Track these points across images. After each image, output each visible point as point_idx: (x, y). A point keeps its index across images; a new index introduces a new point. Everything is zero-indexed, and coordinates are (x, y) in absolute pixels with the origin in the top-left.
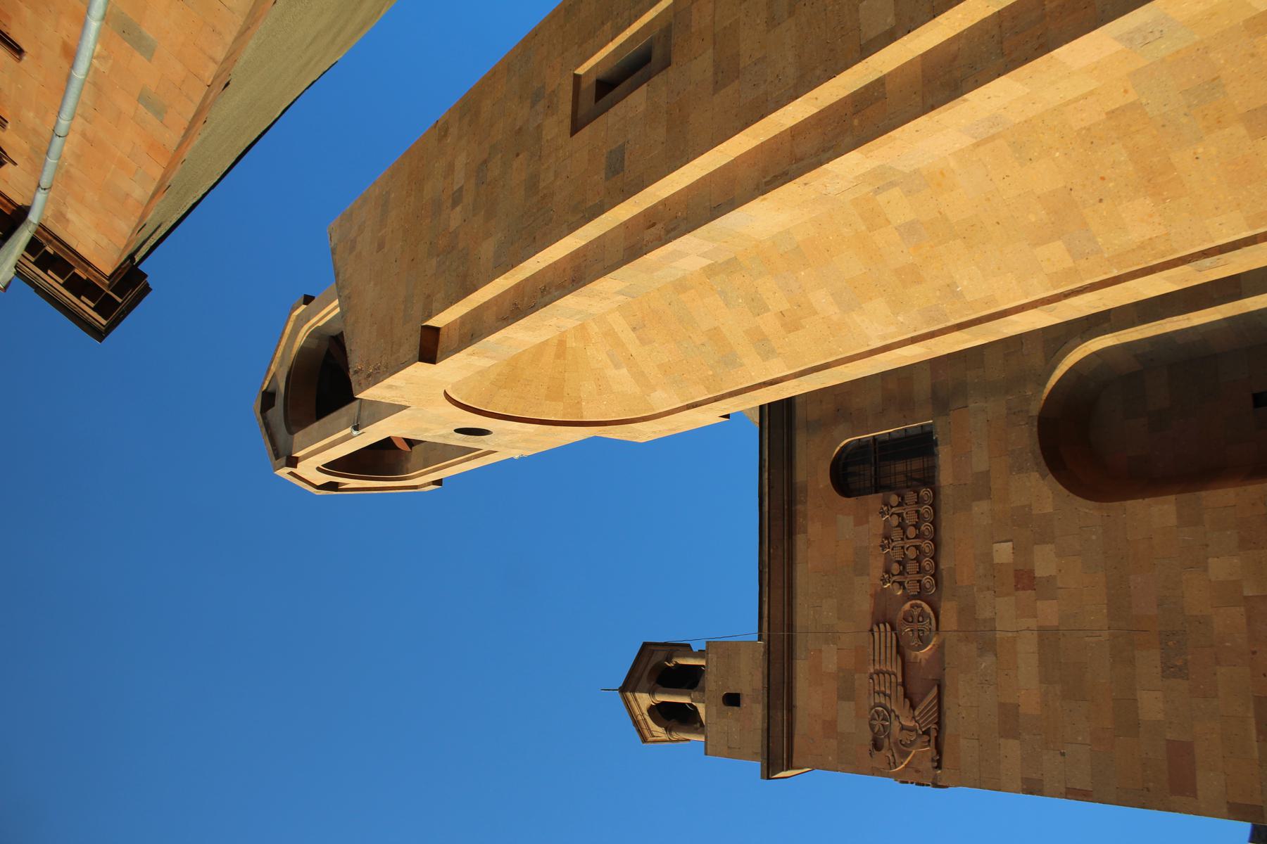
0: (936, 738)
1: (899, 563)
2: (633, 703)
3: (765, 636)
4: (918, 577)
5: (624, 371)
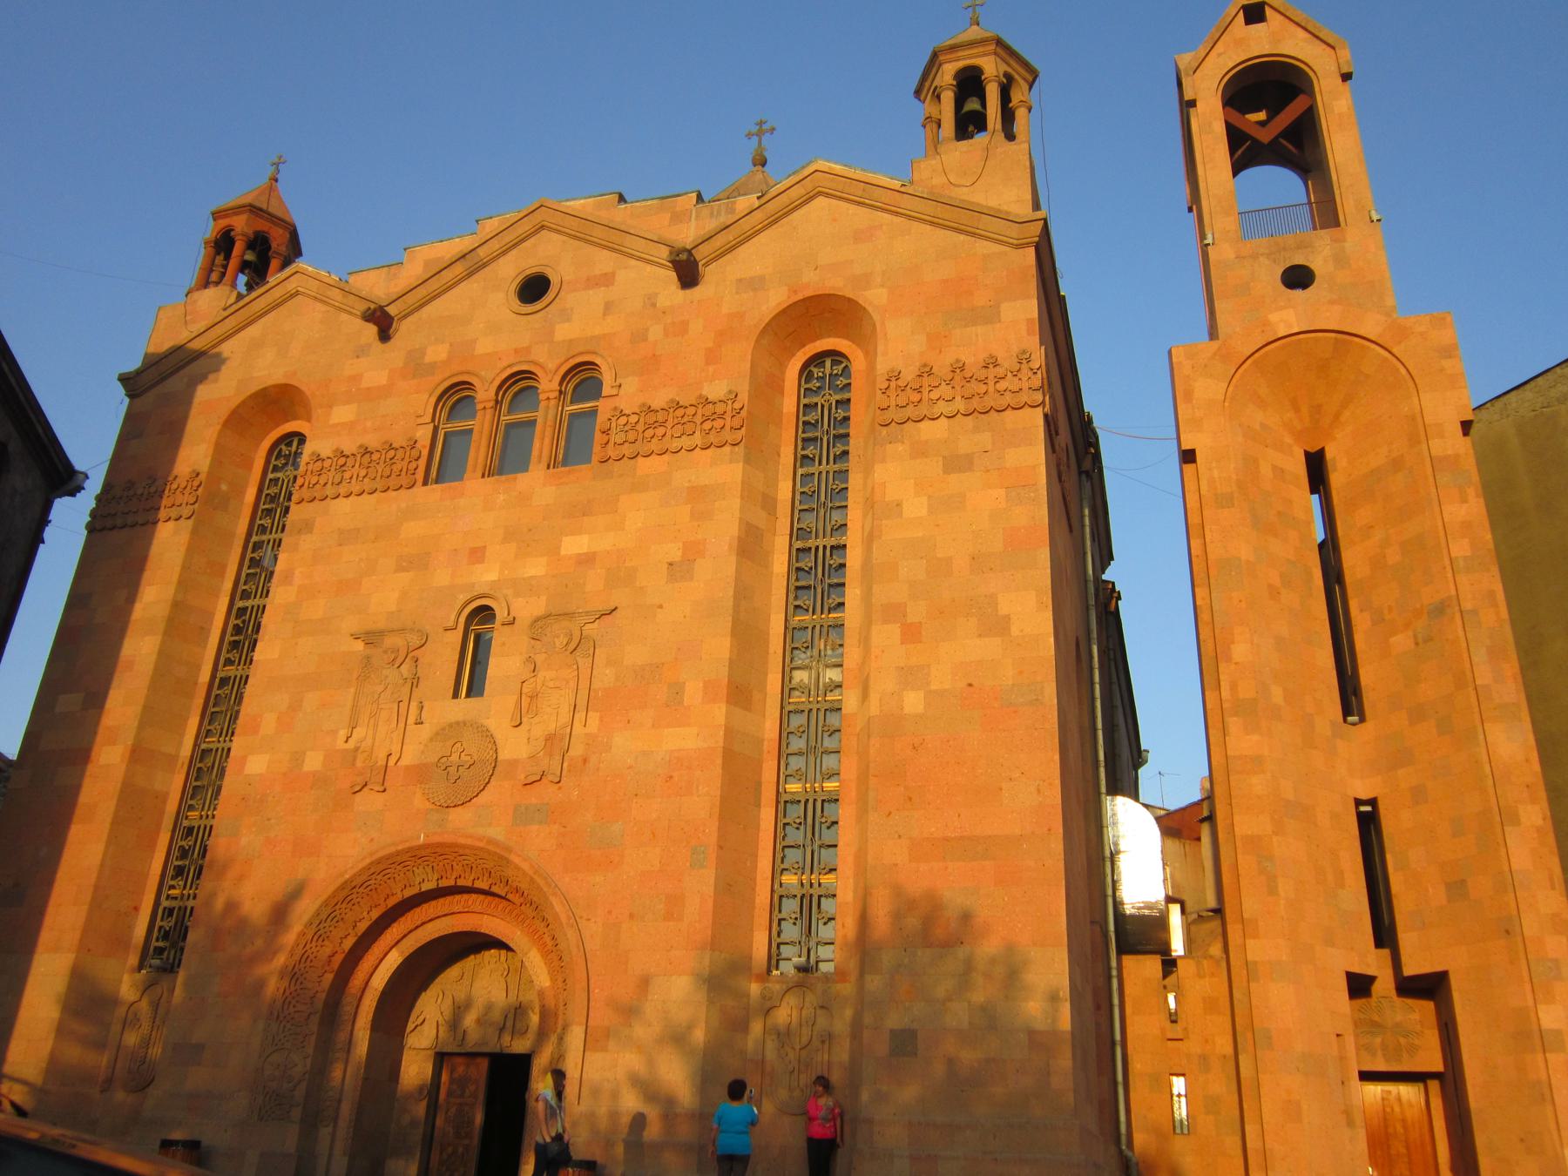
5: (1257, 427)
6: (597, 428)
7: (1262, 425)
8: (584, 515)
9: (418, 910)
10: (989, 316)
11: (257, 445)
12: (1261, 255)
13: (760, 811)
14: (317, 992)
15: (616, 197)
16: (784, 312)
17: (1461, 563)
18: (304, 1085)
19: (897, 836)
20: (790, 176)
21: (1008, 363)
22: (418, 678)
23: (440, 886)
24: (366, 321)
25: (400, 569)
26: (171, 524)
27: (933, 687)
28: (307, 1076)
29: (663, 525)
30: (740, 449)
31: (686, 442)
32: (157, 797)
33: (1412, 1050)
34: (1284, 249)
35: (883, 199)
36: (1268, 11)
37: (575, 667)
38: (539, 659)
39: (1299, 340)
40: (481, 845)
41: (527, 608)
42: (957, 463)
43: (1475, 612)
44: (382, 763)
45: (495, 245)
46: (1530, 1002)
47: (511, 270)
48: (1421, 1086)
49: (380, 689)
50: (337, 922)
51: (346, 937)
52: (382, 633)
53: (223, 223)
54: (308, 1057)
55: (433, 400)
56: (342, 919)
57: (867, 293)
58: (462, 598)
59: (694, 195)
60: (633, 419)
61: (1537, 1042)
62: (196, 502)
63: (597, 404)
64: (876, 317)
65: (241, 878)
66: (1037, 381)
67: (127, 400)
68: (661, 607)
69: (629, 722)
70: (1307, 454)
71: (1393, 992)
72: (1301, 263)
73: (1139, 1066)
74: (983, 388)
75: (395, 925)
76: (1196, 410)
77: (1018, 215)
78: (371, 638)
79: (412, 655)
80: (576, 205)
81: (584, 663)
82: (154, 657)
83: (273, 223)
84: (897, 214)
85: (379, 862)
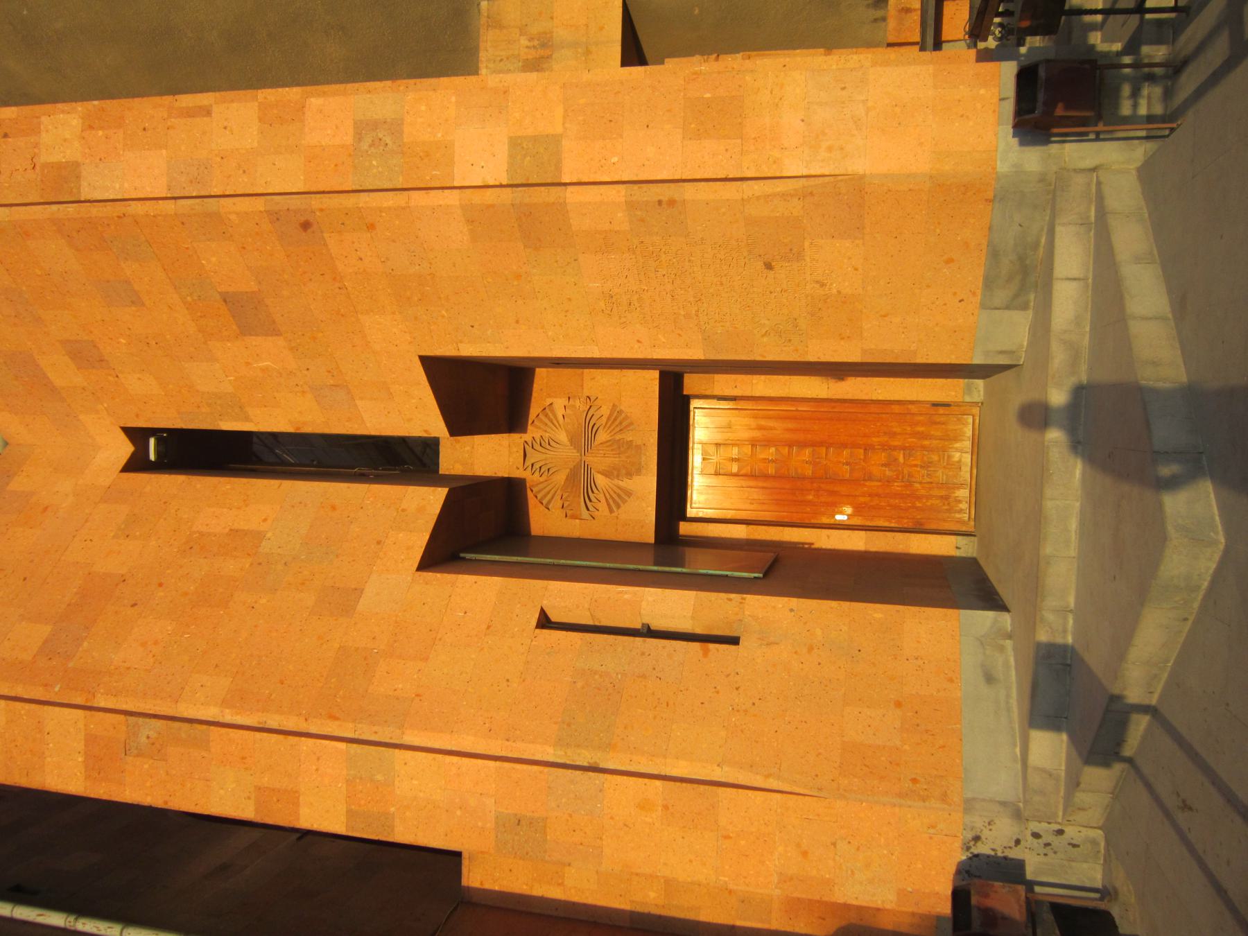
33: (618, 419)
46: (452, 198)
48: (694, 403)
61: (541, 195)
71: (516, 439)
73: (652, 895)
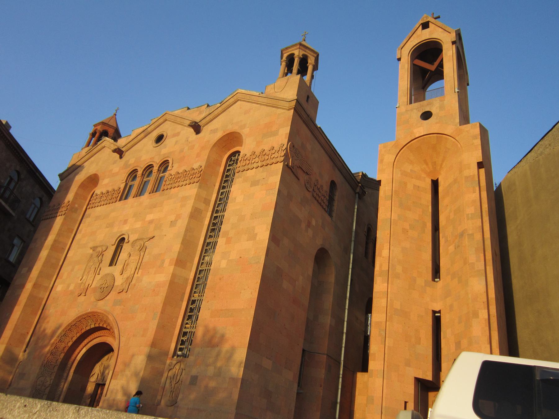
0: (291, 170)
1: (319, 189)
2: (312, 54)
3: (319, 129)
4: (316, 192)
5: (409, 171)
6: (164, 180)
7: (411, 170)
8: (154, 208)
9: (92, 335)
10: (275, 134)
11: (90, 193)
12: (415, 109)
13: (182, 303)
14: (58, 359)
15: (187, 108)
16: (221, 139)
17: (470, 216)
18: (49, 388)
19: (208, 309)
20: (230, 95)
21: (276, 148)
22: (102, 260)
23: (96, 326)
24: (114, 152)
25: (107, 227)
26: (60, 217)
27: (230, 259)
28: (50, 385)
29: (173, 210)
30: (198, 184)
31: (184, 183)
32: (40, 299)
34: (423, 106)
35: (254, 100)
36: (430, 24)
37: (139, 255)
38: (131, 253)
39: (424, 138)
40: (102, 312)
41: (133, 238)
42: (255, 183)
43: (472, 234)
44: (87, 287)
45: (153, 127)
47: (155, 134)
49: (92, 264)
50: (67, 337)
51: (69, 342)
52: (97, 247)
53: (96, 128)
54: (52, 379)
55: (127, 175)
56: (68, 336)
57: (243, 130)
58: (119, 235)
59: (207, 105)
60: (173, 177)
62: (66, 210)
63: (165, 174)
64: (244, 137)
65: (48, 322)
66: (283, 154)
67: (60, 181)
68: (165, 235)
69: (148, 272)
70: (433, 181)
72: (428, 110)
74: (267, 157)
75: (86, 340)
76: (384, 166)
77: (289, 99)
78: (94, 248)
79: (102, 254)
80: (176, 112)
81: (142, 254)
82: (46, 256)
83: (110, 127)
84: (257, 104)
85: (78, 317)
